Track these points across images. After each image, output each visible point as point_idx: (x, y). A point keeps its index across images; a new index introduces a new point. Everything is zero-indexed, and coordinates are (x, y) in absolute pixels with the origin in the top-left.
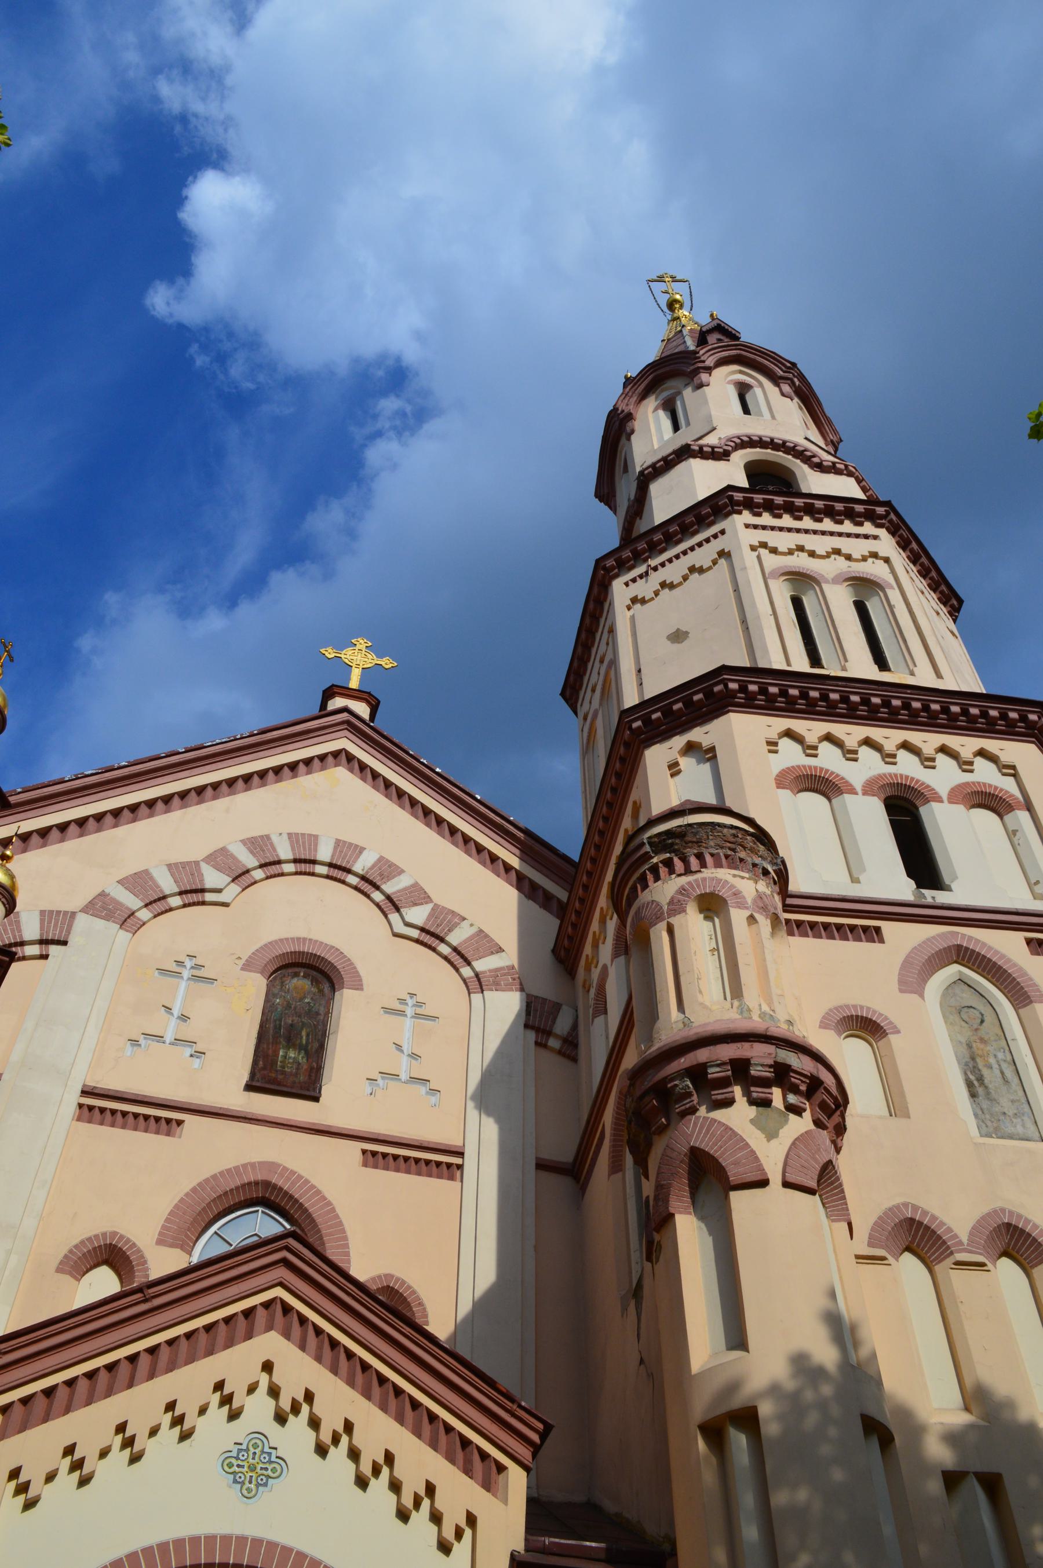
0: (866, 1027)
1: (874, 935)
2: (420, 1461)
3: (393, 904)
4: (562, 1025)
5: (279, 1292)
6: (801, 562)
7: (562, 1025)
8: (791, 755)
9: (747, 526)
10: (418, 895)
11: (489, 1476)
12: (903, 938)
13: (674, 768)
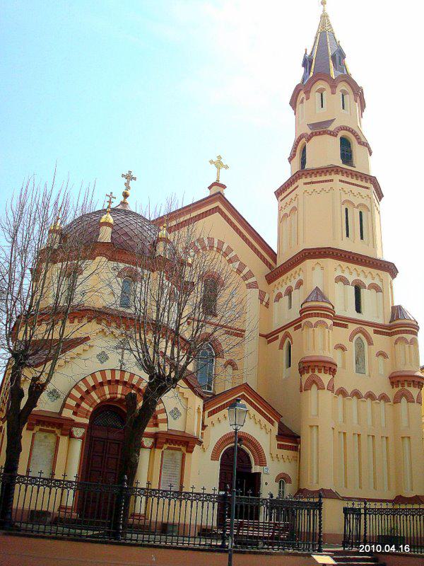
0: (343, 348)
1: (346, 326)
2: (264, 421)
3: (230, 261)
4: (266, 300)
5: (243, 393)
6: (351, 198)
7: (266, 300)
8: (339, 273)
9: (341, 181)
10: (235, 259)
11: (272, 423)
12: (352, 327)
13: (313, 269)
